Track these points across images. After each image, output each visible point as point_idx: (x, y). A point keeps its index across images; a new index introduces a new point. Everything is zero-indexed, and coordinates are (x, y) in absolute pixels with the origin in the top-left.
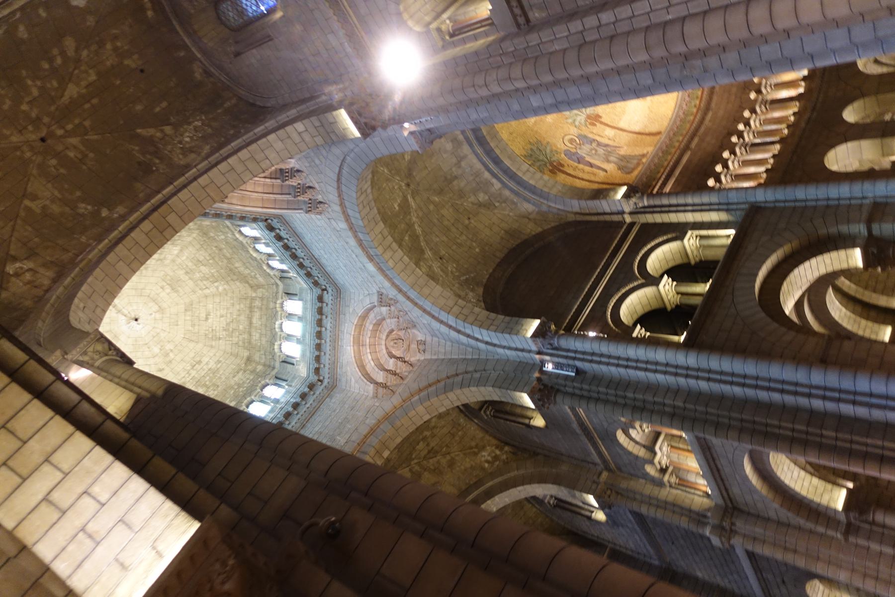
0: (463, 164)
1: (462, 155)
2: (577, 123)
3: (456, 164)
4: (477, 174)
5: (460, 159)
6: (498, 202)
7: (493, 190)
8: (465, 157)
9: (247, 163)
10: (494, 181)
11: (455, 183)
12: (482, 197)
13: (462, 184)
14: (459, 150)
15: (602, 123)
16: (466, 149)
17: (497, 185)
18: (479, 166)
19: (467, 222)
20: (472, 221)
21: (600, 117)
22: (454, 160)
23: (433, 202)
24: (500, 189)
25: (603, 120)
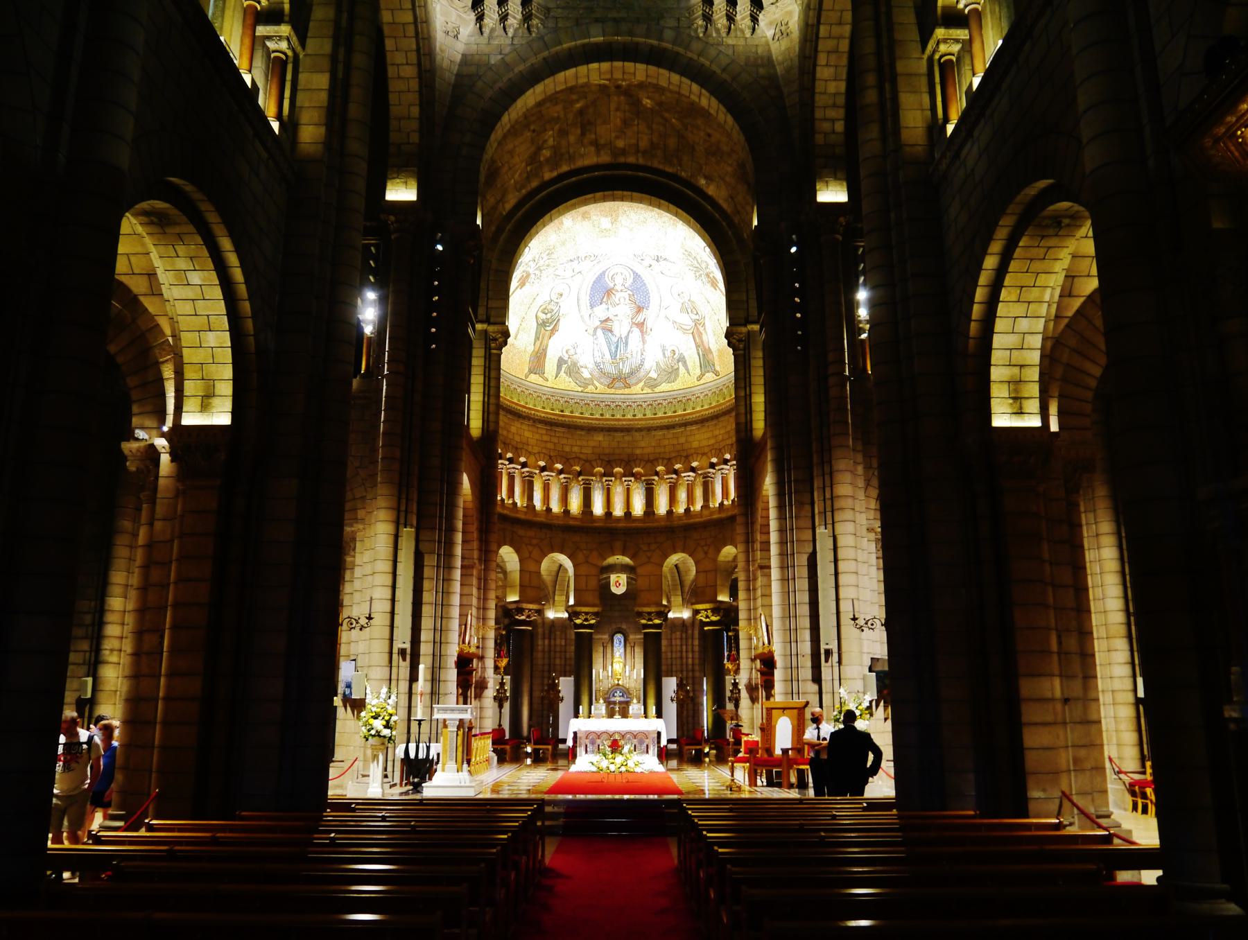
0: (593, 149)
1: (602, 152)
2: (531, 263)
3: (596, 140)
4: (571, 158)
5: (598, 147)
6: (531, 170)
7: (546, 168)
8: (598, 153)
9: (835, 41)
10: (555, 174)
11: (579, 131)
12: (546, 153)
13: (572, 139)
14: (609, 152)
15: (518, 287)
16: (605, 158)
17: (548, 175)
18: (580, 163)
19: (532, 127)
20: (529, 134)
21: (521, 288)
22: (602, 142)
23: (577, 101)
24: (543, 177)
25: (518, 289)
